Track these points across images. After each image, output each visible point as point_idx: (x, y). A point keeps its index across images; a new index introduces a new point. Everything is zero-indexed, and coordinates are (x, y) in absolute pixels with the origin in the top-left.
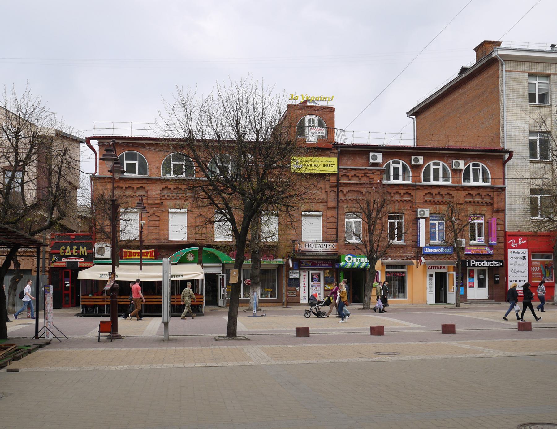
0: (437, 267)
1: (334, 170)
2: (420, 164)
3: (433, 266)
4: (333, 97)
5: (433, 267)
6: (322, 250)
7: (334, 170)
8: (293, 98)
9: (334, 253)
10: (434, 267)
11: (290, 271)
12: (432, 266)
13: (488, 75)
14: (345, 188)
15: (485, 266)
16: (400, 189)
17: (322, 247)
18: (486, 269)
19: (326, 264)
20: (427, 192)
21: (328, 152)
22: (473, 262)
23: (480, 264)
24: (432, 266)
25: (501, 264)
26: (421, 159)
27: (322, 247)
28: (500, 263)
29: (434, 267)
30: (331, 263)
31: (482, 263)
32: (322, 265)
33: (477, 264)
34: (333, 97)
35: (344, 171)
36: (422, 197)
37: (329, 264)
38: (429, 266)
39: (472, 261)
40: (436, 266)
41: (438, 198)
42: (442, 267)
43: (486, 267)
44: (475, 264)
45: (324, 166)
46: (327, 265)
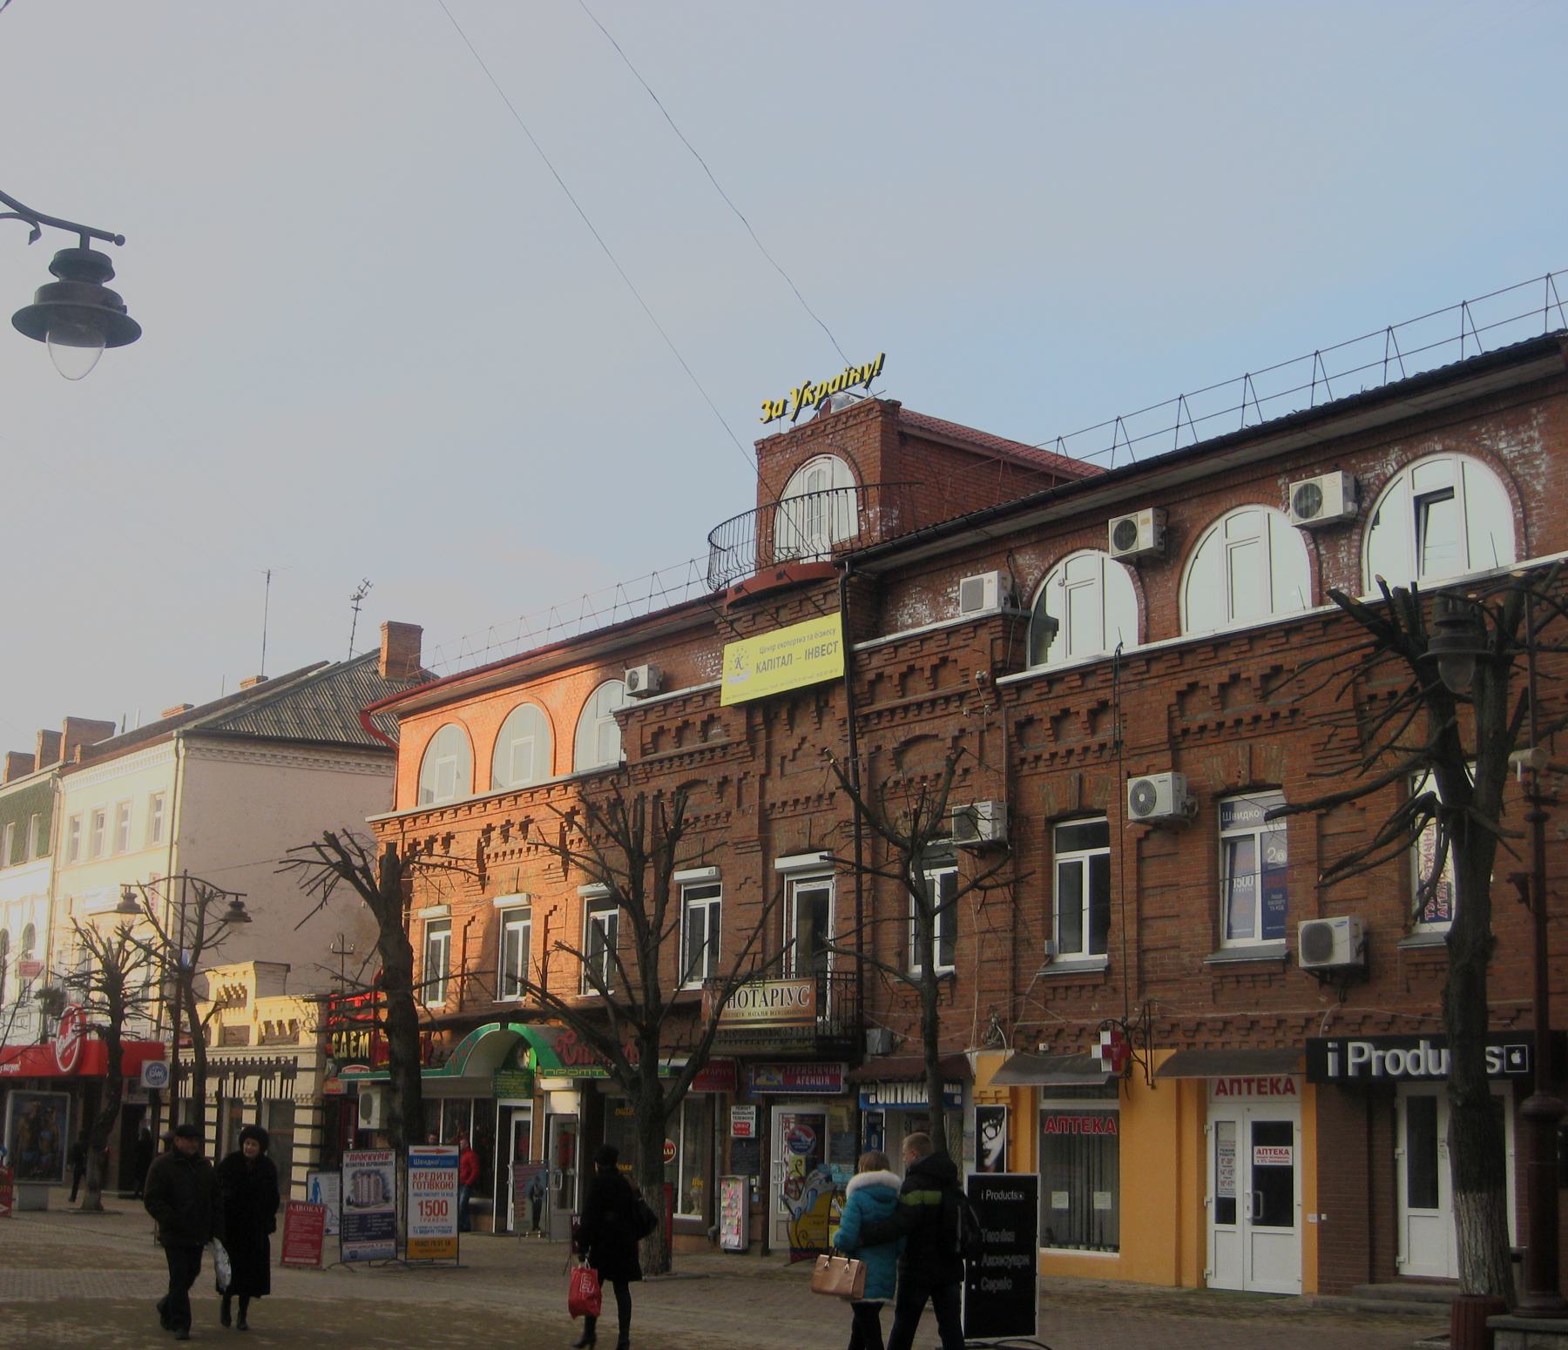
0: (1254, 1086)
1: (833, 666)
2: (1142, 548)
3: (1239, 1081)
4: (883, 356)
5: (1236, 1086)
7: (833, 666)
10: (1244, 1086)
12: (1232, 1082)
14: (889, 734)
15: (1422, 1071)
16: (1072, 692)
18: (1439, 1090)
19: (824, 1074)
20: (1182, 683)
21: (816, 594)
22: (1360, 1052)
23: (1397, 1061)
24: (1232, 1082)
25: (1516, 1058)
26: (1145, 522)
28: (1510, 1051)
31: (1406, 1057)
33: (1383, 1059)
34: (883, 356)
35: (876, 661)
36: (1164, 716)
38: (1222, 1082)
39: (1351, 1045)
41: (1243, 703)
42: (1281, 1086)
43: (1428, 1077)
44: (1368, 1064)
45: (810, 654)
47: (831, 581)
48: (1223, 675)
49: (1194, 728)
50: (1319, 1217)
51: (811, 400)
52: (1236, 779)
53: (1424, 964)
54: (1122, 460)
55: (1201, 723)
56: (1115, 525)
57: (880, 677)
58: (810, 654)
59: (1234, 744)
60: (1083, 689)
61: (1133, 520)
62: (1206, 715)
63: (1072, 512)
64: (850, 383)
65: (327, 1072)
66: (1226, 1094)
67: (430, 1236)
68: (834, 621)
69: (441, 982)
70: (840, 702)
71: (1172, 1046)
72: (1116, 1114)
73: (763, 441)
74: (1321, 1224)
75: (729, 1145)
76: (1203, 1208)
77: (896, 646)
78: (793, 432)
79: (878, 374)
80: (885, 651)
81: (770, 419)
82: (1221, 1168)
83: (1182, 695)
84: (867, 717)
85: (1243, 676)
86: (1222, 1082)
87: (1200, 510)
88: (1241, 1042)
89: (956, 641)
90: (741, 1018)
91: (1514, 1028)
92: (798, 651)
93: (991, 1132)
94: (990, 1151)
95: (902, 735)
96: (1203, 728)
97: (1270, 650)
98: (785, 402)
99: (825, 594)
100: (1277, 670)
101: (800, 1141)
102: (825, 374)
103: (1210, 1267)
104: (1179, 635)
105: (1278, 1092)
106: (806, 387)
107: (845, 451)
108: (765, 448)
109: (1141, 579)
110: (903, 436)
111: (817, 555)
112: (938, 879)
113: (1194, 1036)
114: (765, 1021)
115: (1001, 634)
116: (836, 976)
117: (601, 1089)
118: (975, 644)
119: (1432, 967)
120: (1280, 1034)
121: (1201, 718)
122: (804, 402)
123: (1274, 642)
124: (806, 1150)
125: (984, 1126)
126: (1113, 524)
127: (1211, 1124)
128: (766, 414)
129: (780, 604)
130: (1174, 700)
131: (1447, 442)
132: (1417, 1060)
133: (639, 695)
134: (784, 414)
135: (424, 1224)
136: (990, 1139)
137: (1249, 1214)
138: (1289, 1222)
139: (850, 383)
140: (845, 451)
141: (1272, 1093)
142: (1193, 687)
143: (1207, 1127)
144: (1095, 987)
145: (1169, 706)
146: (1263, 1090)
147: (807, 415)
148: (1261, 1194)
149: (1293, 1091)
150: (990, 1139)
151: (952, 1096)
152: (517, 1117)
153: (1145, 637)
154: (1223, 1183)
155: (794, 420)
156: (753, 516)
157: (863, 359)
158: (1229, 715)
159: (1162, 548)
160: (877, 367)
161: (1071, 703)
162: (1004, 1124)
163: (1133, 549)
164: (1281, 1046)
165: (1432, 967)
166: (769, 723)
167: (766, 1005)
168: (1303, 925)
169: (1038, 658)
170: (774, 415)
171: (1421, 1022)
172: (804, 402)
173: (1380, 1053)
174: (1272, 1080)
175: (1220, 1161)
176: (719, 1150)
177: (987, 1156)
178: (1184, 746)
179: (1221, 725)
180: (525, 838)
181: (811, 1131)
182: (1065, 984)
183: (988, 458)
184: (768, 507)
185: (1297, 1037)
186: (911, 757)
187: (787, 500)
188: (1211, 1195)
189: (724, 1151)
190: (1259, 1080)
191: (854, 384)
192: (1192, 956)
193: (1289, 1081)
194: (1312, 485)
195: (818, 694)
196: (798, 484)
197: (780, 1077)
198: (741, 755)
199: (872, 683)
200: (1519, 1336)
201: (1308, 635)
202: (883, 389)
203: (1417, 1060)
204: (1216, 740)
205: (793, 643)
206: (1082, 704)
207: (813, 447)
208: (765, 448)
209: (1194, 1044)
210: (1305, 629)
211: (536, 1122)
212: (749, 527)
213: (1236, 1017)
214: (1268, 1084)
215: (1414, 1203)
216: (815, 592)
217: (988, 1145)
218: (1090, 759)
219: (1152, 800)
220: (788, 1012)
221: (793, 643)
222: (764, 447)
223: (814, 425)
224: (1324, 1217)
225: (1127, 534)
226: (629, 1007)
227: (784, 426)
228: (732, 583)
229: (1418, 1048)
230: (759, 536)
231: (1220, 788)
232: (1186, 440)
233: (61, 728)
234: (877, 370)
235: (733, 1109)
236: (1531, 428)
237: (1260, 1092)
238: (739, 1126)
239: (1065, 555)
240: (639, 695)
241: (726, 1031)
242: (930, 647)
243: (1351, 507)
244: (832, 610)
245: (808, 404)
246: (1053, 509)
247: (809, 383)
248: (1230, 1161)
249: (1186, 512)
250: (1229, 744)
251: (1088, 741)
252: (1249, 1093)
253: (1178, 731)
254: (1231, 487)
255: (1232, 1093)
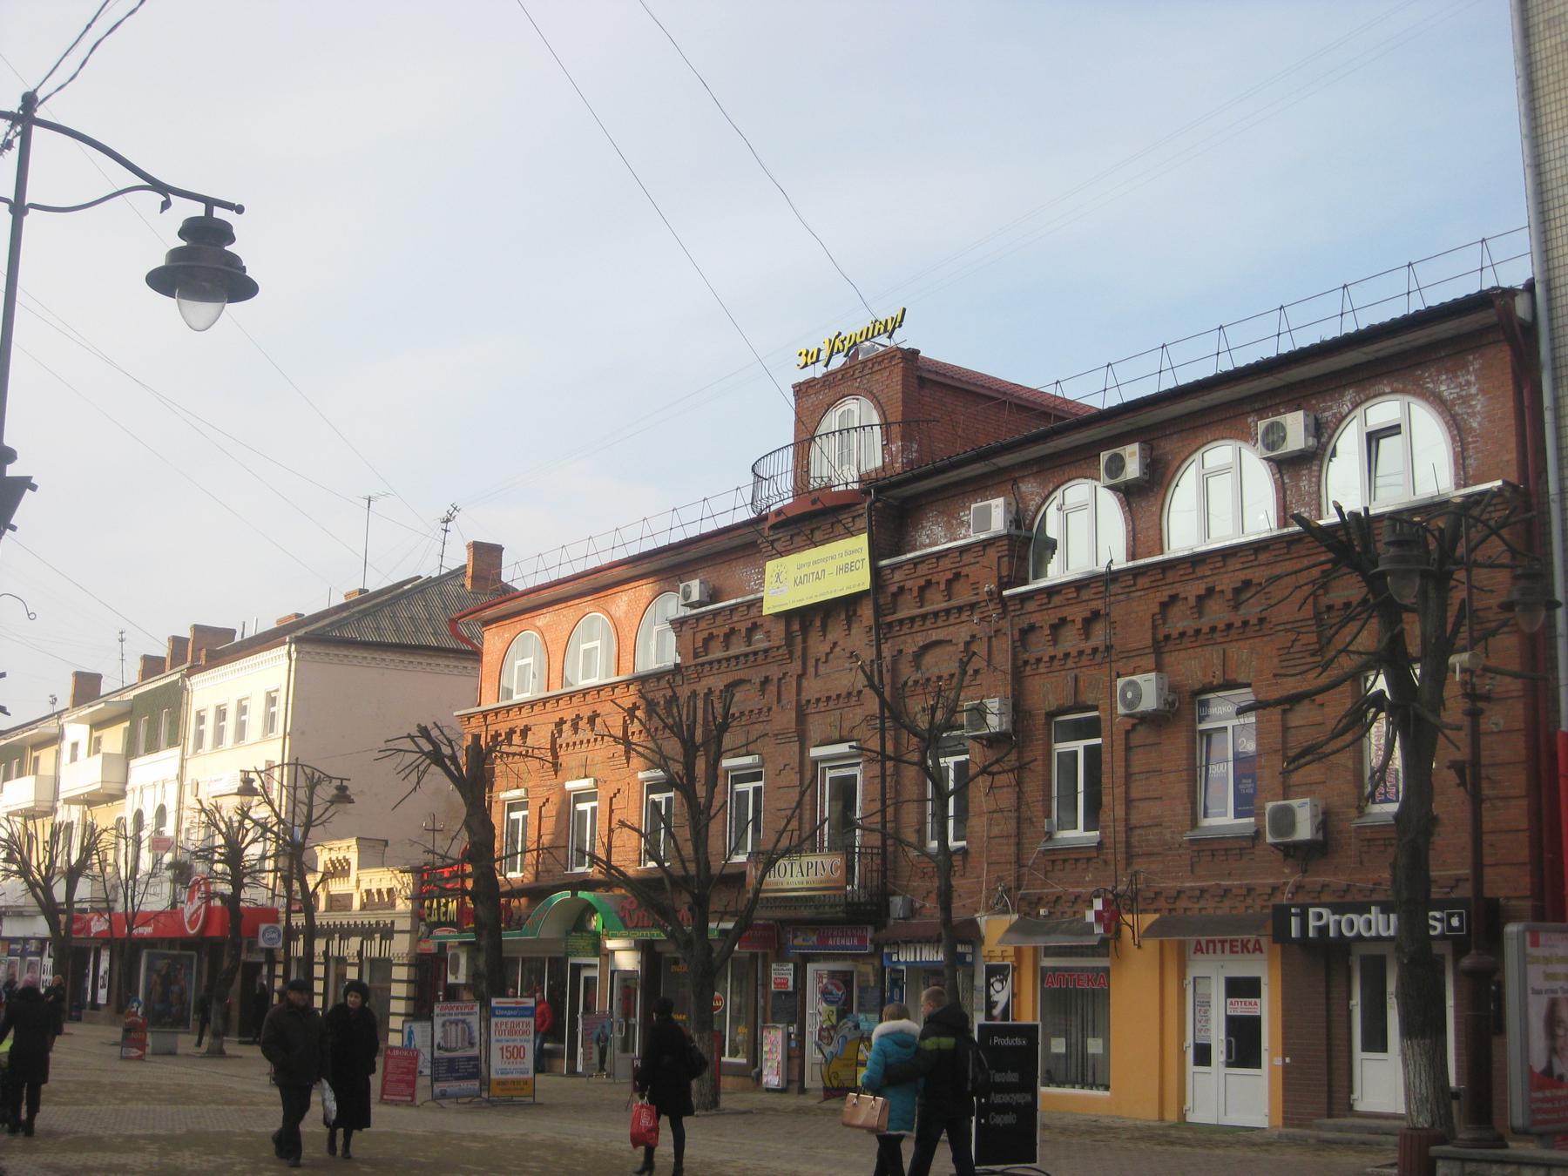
0: (1227, 946)
1: (860, 580)
3: (1213, 942)
4: (904, 310)
7: (860, 580)
8: (811, 358)
10: (1219, 946)
12: (1208, 942)
15: (1373, 933)
16: (1069, 603)
18: (1387, 950)
19: (853, 936)
20: (1164, 596)
21: (846, 518)
22: (1319, 916)
23: (1351, 925)
24: (1208, 942)
25: (1455, 922)
26: (1132, 454)
28: (1450, 916)
29: (1219, 946)
31: (1359, 921)
33: (1339, 922)
34: (904, 310)
35: (898, 576)
36: (1148, 624)
39: (1312, 911)
40: (1223, 942)
41: (1217, 612)
42: (1251, 946)
43: (1379, 938)
44: (1326, 927)
45: (840, 570)
47: (858, 507)
48: (1199, 588)
49: (1175, 634)
50: (1284, 1060)
51: (841, 348)
52: (1211, 679)
53: (1374, 840)
54: (1112, 400)
55: (1181, 630)
56: (1106, 458)
57: (902, 589)
58: (840, 570)
59: (1210, 648)
60: (1078, 601)
61: (1122, 453)
62: (1185, 623)
63: (1068, 446)
64: (876, 333)
65: (420, 934)
66: (1202, 952)
67: (510, 1076)
68: (862, 541)
69: (519, 856)
70: (866, 612)
71: (1156, 911)
72: (1107, 970)
73: (800, 384)
74: (1285, 1066)
75: (770, 997)
76: (1182, 1053)
77: (915, 562)
78: (826, 376)
79: (900, 326)
80: (906, 567)
81: (806, 365)
82: (1198, 1017)
83: (1164, 606)
84: (890, 625)
85: (1217, 589)
86: (1199, 942)
87: (1180, 444)
88: (1216, 908)
89: (967, 558)
90: (780, 887)
91: (1453, 896)
92: (831, 567)
93: (998, 986)
94: (997, 1002)
95: (921, 640)
96: (1182, 635)
97: (1241, 566)
98: (819, 350)
99: (854, 518)
100: (1247, 584)
101: (831, 993)
102: (854, 325)
103: (1189, 1104)
104: (1162, 553)
105: (1248, 952)
106: (837, 337)
107: (871, 393)
108: (801, 390)
109: (1129, 505)
110: (922, 381)
111: (847, 484)
112: (952, 766)
113: (1174, 903)
115: (1007, 553)
116: (863, 850)
117: (658, 948)
118: (985, 561)
119: (1382, 842)
120: (1249, 901)
121: (1181, 626)
122: (835, 350)
123: (1244, 559)
124: (837, 1002)
125: (992, 981)
126: (1104, 456)
127: (1189, 979)
128: (802, 360)
129: (814, 526)
130: (1157, 610)
131: (1395, 385)
132: (1369, 923)
133: (692, 606)
134: (817, 360)
135: (504, 1067)
136: (997, 992)
137: (1223, 1058)
138: (1258, 1065)
139: (876, 333)
140: (871, 393)
141: (1243, 952)
142: (1174, 598)
143: (1186, 982)
144: (1089, 859)
145: (1153, 615)
146: (1235, 949)
147: (838, 361)
148: (1233, 1039)
149: (1261, 950)
150: (997, 992)
151: (964, 955)
152: (585, 973)
153: (1132, 555)
154: (1200, 1030)
155: (826, 366)
156: (791, 449)
157: (887, 313)
158: (1205, 623)
159: (1147, 477)
160: (899, 320)
161: (1067, 612)
162: (1010, 979)
163: (1122, 479)
164: (1250, 911)
165: (1382, 842)
166: (805, 630)
168: (1269, 806)
169: (1040, 572)
170: (809, 362)
171: (1372, 891)
172: (835, 350)
173: (1337, 917)
174: (1242, 941)
175: (1197, 1011)
176: (761, 1002)
177: (994, 1007)
178: (1166, 650)
179: (1198, 632)
180: (592, 730)
181: (841, 985)
182: (1062, 857)
183: (996, 399)
184: (804, 441)
185: (1265, 904)
186: (929, 659)
187: (820, 436)
188: (1189, 1041)
189: (766, 1003)
190: (1232, 941)
191: (879, 334)
192: (1173, 832)
193: (1257, 942)
194: (1278, 423)
195: (848, 604)
196: (832, 421)
197: (815, 938)
198: (780, 658)
199: (895, 595)
200: (1458, 1164)
201: (1274, 553)
202: (905, 338)
203: (1369, 923)
204: (1194, 645)
205: (824, 560)
206: (1077, 613)
207: (843, 389)
208: (801, 390)
209: (1174, 909)
210: (1271, 547)
211: (602, 977)
212: (787, 459)
213: (1212, 886)
214: (1239, 944)
215: (1366, 1048)
216: (845, 516)
217: (995, 998)
218: (1085, 660)
219: (1138, 697)
220: (821, 882)
221: (824, 560)
222: (800, 390)
223: (843, 370)
224: (1288, 1060)
225: (1117, 465)
226: (683, 877)
227: (818, 371)
228: (773, 508)
229: (1370, 913)
230: (796, 468)
231: (1197, 686)
232: (1168, 383)
233: (187, 633)
234: (899, 322)
235: (774, 966)
236: (1468, 373)
237: (1232, 952)
238: (779, 981)
239: (1063, 484)
240: (692, 606)
241: (767, 898)
242: (945, 563)
243: (1312, 441)
244: (860, 531)
245: (838, 352)
246: (1052, 444)
247: (840, 334)
248: (1206, 1011)
249: (1167, 446)
250: (1205, 648)
251: (1082, 645)
252: (1223, 952)
253: (1160, 637)
254: (1206, 424)
255: (1208, 952)
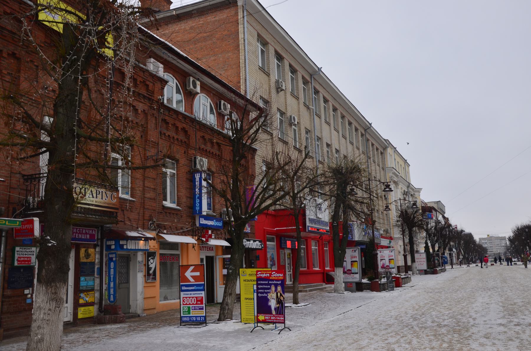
6: (94, 203)
9: (110, 212)
11: (17, 249)
13: (217, 18)
17: (95, 195)
19: (86, 233)
27: (95, 195)
30: (94, 233)
32: (80, 236)
37: (91, 235)
46: (88, 236)
93: (152, 261)
94: (151, 268)
114: (92, 205)
136: (152, 263)
150: (152, 263)
151: (123, 245)
167: (93, 197)
177: (150, 270)
182: (169, 211)
217: (151, 266)
220: (105, 203)
238: (22, 259)
241: (81, 208)
